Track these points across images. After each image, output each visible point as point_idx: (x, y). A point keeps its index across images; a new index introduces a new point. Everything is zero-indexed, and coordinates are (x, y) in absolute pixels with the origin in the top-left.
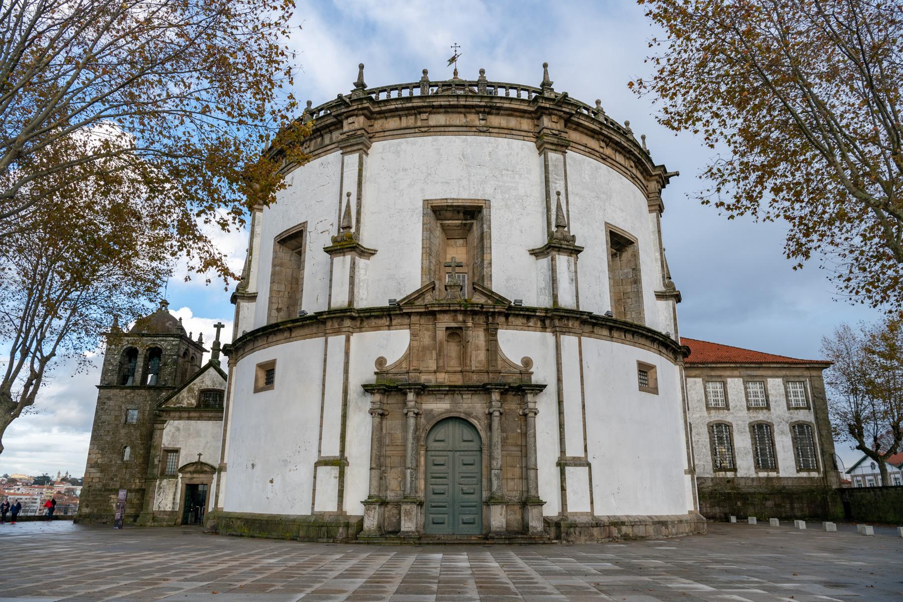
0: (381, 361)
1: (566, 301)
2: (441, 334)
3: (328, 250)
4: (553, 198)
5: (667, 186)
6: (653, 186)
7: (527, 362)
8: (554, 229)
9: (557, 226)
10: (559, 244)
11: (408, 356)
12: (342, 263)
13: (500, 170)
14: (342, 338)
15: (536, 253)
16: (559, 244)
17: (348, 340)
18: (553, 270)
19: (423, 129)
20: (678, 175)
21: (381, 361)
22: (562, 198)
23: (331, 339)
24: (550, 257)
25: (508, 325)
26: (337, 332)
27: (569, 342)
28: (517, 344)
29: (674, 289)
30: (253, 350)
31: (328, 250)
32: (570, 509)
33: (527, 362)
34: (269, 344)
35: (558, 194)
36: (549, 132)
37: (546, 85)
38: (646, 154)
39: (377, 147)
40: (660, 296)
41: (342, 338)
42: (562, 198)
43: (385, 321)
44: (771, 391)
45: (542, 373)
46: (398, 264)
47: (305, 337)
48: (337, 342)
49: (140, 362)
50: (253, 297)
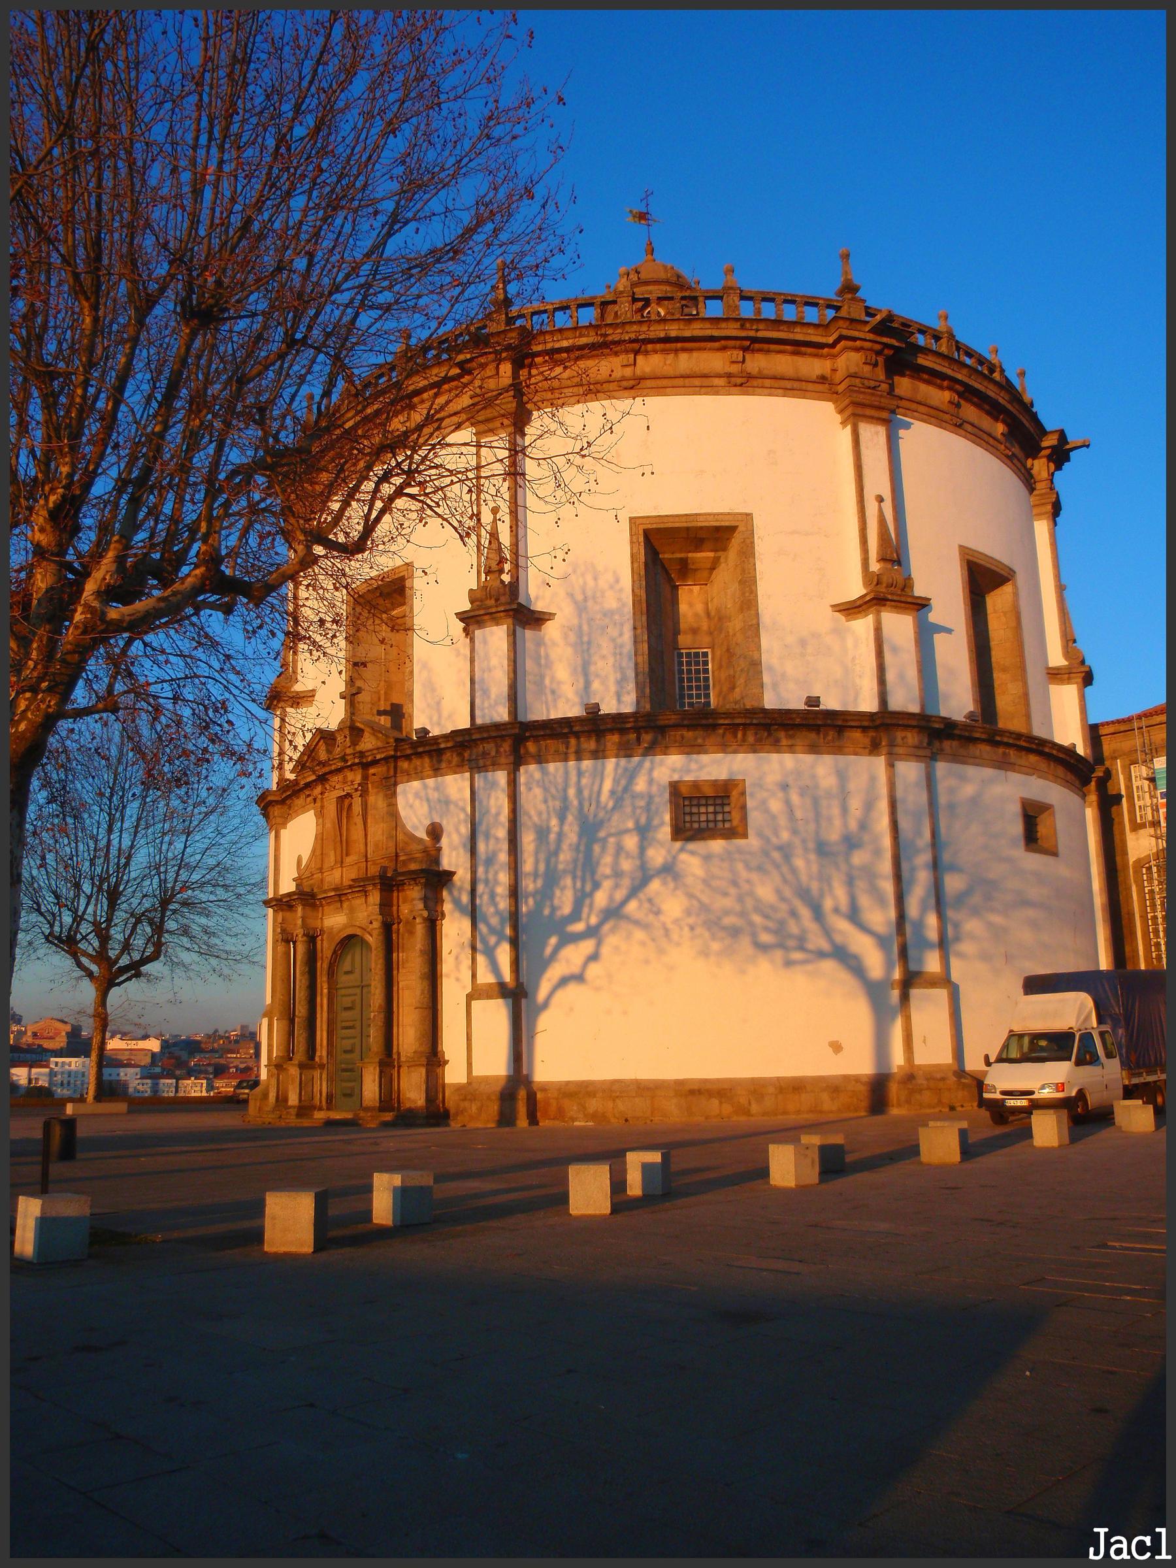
3: (463, 617)
5: (1066, 466)
6: (1040, 467)
8: (875, 567)
9: (882, 559)
14: (501, 777)
17: (513, 783)
19: (625, 384)
20: (1088, 446)
24: (870, 619)
29: (1083, 662)
31: (463, 617)
32: (918, 1061)
35: (880, 499)
36: (857, 382)
37: (849, 288)
38: (1027, 408)
40: (1055, 675)
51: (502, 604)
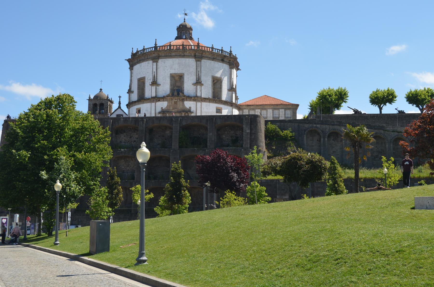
0: (162, 108)
1: (199, 94)
2: (173, 103)
4: (198, 72)
7: (190, 108)
10: (198, 82)
11: (167, 107)
12: (154, 88)
13: (186, 66)
14: (154, 103)
15: (194, 84)
16: (198, 82)
18: (196, 89)
21: (162, 108)
22: (200, 72)
23: (152, 104)
25: (186, 100)
26: (153, 102)
27: (199, 104)
28: (188, 104)
30: (135, 105)
33: (190, 108)
34: (139, 104)
39: (160, 61)
41: (154, 103)
42: (200, 72)
43: (162, 100)
44: (280, 113)
45: (193, 109)
46: (165, 88)
47: (146, 103)
48: (153, 104)
49: (98, 107)
50: (133, 92)
51: (155, 83)
